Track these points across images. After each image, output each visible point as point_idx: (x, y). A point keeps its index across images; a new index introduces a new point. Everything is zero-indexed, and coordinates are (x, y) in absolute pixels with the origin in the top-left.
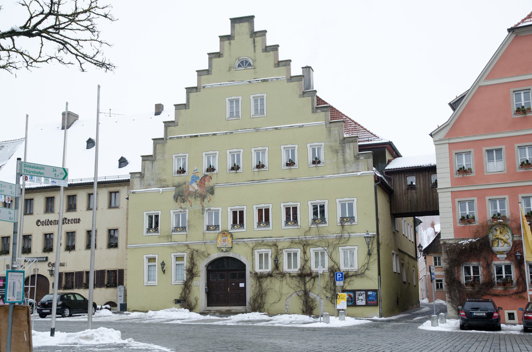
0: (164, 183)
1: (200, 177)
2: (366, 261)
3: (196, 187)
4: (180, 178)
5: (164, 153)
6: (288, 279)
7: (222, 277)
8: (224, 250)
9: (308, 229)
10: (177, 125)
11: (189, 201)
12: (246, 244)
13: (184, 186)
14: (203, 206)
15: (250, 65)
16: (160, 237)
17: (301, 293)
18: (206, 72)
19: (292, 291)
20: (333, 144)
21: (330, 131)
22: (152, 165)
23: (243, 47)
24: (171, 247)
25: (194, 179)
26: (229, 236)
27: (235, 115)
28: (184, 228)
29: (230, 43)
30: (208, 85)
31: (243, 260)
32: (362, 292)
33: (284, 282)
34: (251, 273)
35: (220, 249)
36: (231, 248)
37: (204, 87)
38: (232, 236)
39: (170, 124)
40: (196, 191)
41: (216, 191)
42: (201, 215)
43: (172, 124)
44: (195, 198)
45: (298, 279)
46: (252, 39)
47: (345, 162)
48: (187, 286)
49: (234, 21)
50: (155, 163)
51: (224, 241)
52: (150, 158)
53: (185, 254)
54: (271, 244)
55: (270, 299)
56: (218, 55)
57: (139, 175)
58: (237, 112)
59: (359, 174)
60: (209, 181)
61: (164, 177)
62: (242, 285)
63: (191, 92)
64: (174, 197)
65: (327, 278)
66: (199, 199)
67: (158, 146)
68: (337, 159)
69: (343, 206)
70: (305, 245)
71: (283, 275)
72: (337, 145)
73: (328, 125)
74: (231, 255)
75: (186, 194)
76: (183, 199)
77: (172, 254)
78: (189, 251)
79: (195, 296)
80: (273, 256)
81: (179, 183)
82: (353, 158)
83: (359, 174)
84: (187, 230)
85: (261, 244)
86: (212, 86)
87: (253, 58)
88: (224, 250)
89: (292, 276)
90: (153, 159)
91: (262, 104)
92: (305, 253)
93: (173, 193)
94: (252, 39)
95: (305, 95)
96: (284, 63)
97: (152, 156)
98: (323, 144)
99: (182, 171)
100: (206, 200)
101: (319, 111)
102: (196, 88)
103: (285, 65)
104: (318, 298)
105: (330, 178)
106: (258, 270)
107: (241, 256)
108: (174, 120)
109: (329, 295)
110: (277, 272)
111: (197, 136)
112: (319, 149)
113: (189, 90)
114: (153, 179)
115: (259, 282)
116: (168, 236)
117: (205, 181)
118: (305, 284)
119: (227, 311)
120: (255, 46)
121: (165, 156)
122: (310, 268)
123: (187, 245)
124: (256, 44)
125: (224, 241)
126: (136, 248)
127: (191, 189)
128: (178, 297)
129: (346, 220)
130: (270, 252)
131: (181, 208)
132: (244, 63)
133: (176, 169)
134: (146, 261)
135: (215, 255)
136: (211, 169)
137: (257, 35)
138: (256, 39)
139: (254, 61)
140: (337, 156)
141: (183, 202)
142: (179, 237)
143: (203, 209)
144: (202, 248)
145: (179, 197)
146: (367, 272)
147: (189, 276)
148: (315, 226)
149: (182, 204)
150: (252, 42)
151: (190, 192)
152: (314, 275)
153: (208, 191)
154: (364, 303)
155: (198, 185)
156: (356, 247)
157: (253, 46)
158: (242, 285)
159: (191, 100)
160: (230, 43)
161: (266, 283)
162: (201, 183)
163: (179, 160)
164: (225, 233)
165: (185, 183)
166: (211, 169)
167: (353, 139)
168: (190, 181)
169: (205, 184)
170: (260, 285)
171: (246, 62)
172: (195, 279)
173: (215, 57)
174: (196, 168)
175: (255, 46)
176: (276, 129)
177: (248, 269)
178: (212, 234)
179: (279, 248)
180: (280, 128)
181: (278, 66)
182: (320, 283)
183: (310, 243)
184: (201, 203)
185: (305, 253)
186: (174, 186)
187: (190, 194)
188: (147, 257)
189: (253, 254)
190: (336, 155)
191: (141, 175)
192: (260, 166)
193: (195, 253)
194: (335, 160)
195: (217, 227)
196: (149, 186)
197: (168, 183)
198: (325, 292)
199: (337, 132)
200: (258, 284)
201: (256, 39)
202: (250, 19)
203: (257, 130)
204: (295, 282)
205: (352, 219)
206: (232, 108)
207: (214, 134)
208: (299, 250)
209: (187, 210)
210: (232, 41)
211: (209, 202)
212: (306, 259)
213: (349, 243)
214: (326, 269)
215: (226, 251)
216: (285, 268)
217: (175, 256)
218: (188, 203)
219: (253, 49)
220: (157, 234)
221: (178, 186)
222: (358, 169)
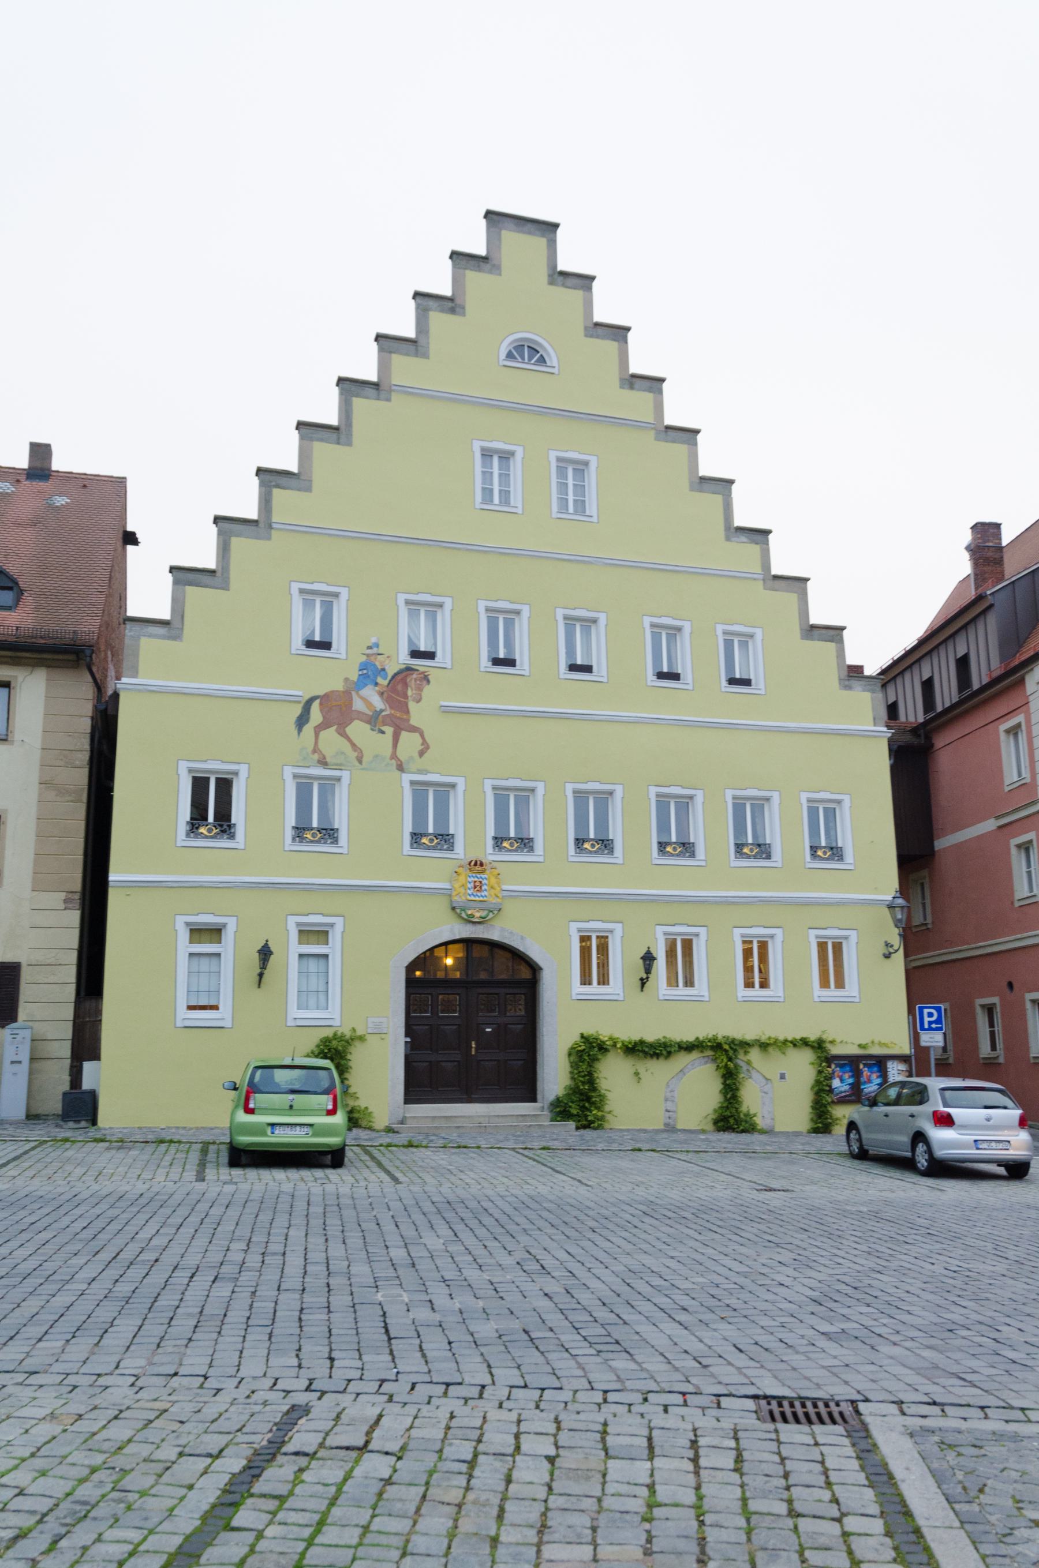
3: (378, 703)
25: (369, 672)
31: (535, 952)
58: (505, 495)
101: (743, 539)
117: (406, 685)
155: (381, 694)
163: (308, 605)
174: (374, 640)
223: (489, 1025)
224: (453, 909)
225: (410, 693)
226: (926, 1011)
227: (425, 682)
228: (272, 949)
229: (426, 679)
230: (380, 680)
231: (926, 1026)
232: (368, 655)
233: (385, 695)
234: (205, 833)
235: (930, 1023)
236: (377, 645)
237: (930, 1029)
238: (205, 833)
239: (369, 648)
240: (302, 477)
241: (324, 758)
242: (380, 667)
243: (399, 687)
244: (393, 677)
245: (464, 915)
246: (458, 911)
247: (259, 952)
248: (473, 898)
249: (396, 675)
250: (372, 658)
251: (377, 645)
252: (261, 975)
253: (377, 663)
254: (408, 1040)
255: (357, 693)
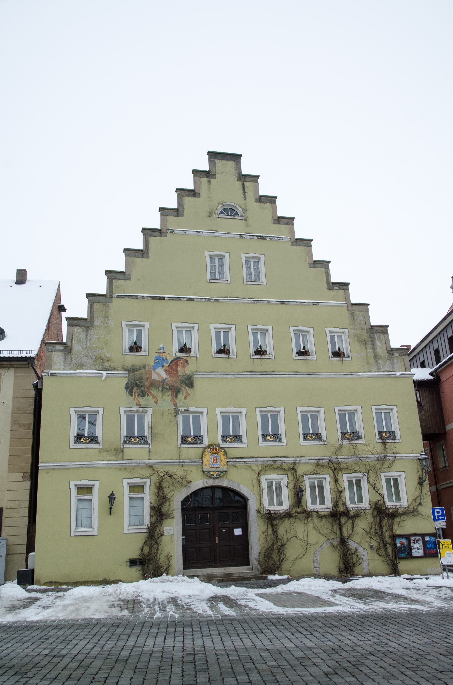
0: (107, 364)
1: (170, 359)
2: (418, 493)
3: (164, 375)
4: (133, 359)
5: (107, 317)
6: (316, 520)
7: (204, 519)
8: (215, 475)
9: (337, 446)
10: (129, 279)
11: (153, 395)
12: (248, 467)
13: (143, 371)
14: (176, 405)
15: (236, 214)
16: (101, 451)
17: (336, 542)
18: (175, 212)
19: (322, 539)
20: (358, 332)
21: (353, 315)
22: (87, 333)
23: (225, 189)
24: (123, 468)
25: (160, 361)
26: (223, 453)
27: (218, 277)
28: (142, 439)
29: (209, 182)
30: (179, 230)
31: (245, 491)
32: (417, 538)
33: (310, 526)
34: (258, 511)
35: (206, 474)
36: (226, 471)
37: (172, 232)
38: (225, 454)
39: (117, 276)
40: (164, 380)
41: (197, 383)
42: (173, 419)
43: (122, 276)
44: (162, 391)
45: (330, 520)
46: (240, 183)
47: (376, 357)
48: (153, 536)
49: (213, 156)
50: (92, 332)
51: (215, 461)
52: (83, 323)
53: (148, 481)
54: (286, 468)
55: (292, 552)
56: (193, 193)
57: (62, 348)
59: (398, 374)
60: (184, 367)
61: (108, 355)
62: (238, 532)
63: (151, 236)
64: (127, 387)
65: (370, 519)
66: (170, 393)
67: (96, 306)
68: (367, 352)
69: (225, 419)
70: (336, 469)
71: (307, 514)
72: (364, 334)
73: (350, 308)
74: (224, 483)
75: (147, 384)
76: (142, 392)
77: (125, 481)
78: (155, 477)
79: (166, 552)
80: (291, 486)
81: (133, 366)
82: (385, 353)
83: (398, 374)
84: (150, 441)
85: (271, 466)
86: (185, 232)
87: (243, 207)
88: (215, 475)
89: (320, 516)
90: (88, 324)
91: (257, 269)
92: (336, 481)
93: (125, 381)
94: (240, 183)
95: (317, 265)
96: (286, 221)
97: (85, 319)
98: (346, 331)
99: (135, 348)
100: (181, 396)
102: (159, 231)
103: (287, 224)
104: (361, 550)
105: (360, 377)
106: (267, 506)
107: (241, 486)
108: (123, 270)
109: (375, 544)
110: (299, 510)
111: (163, 298)
112: (340, 337)
113: (148, 232)
114: (87, 356)
115: (272, 525)
116: (116, 450)
117: (177, 365)
118: (341, 527)
119: (225, 575)
120: (245, 193)
121: (109, 322)
122: (344, 504)
123: (151, 466)
124: (246, 190)
125: (215, 461)
126: (54, 469)
127: (155, 377)
128: (135, 555)
129: (386, 436)
130: (284, 480)
131: (139, 405)
132: (230, 211)
133: (127, 344)
134: (74, 491)
135: (199, 482)
136: (184, 349)
137: (247, 179)
138: (245, 183)
139: (245, 210)
140: (366, 348)
141: (143, 396)
142: (136, 451)
143: (176, 410)
144: (179, 472)
145: (135, 388)
146: (420, 509)
147: (154, 518)
148: (348, 442)
149: (142, 401)
150: (241, 186)
151: (154, 380)
152: (352, 513)
153: (183, 382)
154: (421, 553)
155: (166, 371)
156: (403, 474)
157: (242, 191)
158: (238, 532)
159: (151, 247)
160: (209, 182)
161: (284, 528)
162: (172, 368)
163: (131, 331)
164: (213, 447)
165: (144, 367)
166: (184, 349)
167: (382, 329)
168: (152, 363)
169: (177, 371)
170: (275, 532)
171: (232, 210)
172: (166, 522)
173: (188, 195)
174: (161, 346)
175: (245, 193)
176: (282, 303)
177: (253, 507)
178: (192, 451)
179: (300, 472)
180: (288, 304)
181: (279, 223)
182: (362, 525)
183: (344, 465)
184: (172, 400)
185: (336, 481)
186: (126, 370)
187: (153, 384)
188: (76, 486)
189: (259, 482)
190: (364, 347)
191: (66, 347)
192: (260, 352)
193: (167, 478)
194: (364, 354)
195: (198, 439)
196: (81, 366)
197: (114, 365)
198: (368, 539)
199: (361, 318)
200: (270, 531)
201: (245, 183)
202: (236, 158)
203: (256, 302)
204: (326, 526)
205: (392, 434)
206: (213, 267)
207: (190, 299)
208: (327, 477)
209: (149, 410)
210: (212, 180)
211: (185, 398)
212: (340, 489)
213: (394, 467)
214: (366, 503)
215: (219, 477)
216: (308, 502)
217: (128, 483)
218: (150, 398)
219: (242, 196)
220: (97, 446)
221: (132, 370)
222: (393, 368)
223: (224, 528)
224: (203, 472)
225: (179, 369)
226: (436, 511)
227: (186, 364)
228: (116, 495)
229: (187, 362)
230: (164, 364)
231: (437, 518)
232: (159, 353)
233: (168, 371)
234: (84, 441)
235: (438, 516)
236: (163, 348)
237: (439, 519)
238: (84, 441)
239: (159, 349)
240: (126, 274)
241: (139, 402)
242: (164, 358)
243: (174, 367)
244: (171, 363)
245: (209, 475)
246: (206, 473)
247: (109, 497)
248: (213, 466)
249: (172, 361)
250: (161, 354)
251: (163, 348)
252: (111, 508)
253: (163, 357)
254: (184, 537)
255: (154, 371)
